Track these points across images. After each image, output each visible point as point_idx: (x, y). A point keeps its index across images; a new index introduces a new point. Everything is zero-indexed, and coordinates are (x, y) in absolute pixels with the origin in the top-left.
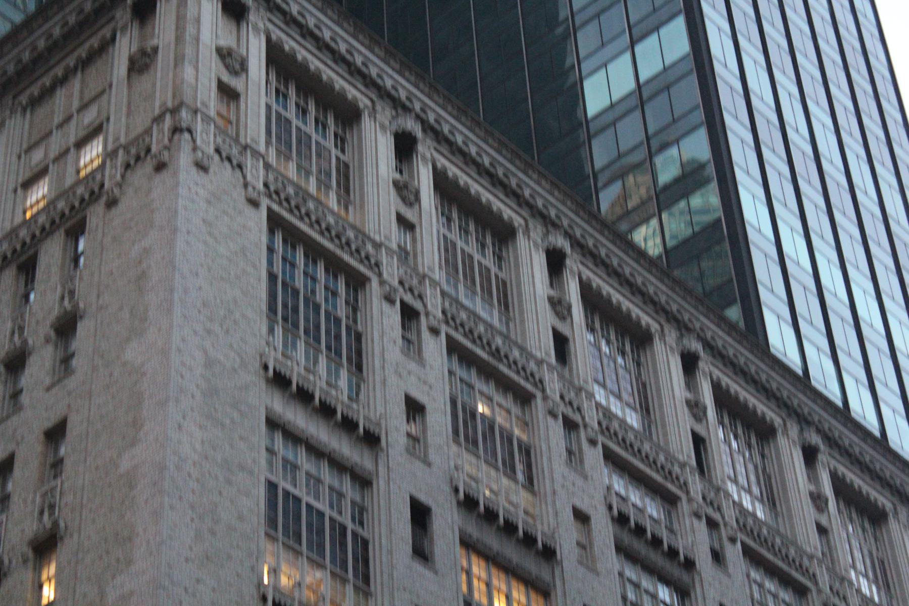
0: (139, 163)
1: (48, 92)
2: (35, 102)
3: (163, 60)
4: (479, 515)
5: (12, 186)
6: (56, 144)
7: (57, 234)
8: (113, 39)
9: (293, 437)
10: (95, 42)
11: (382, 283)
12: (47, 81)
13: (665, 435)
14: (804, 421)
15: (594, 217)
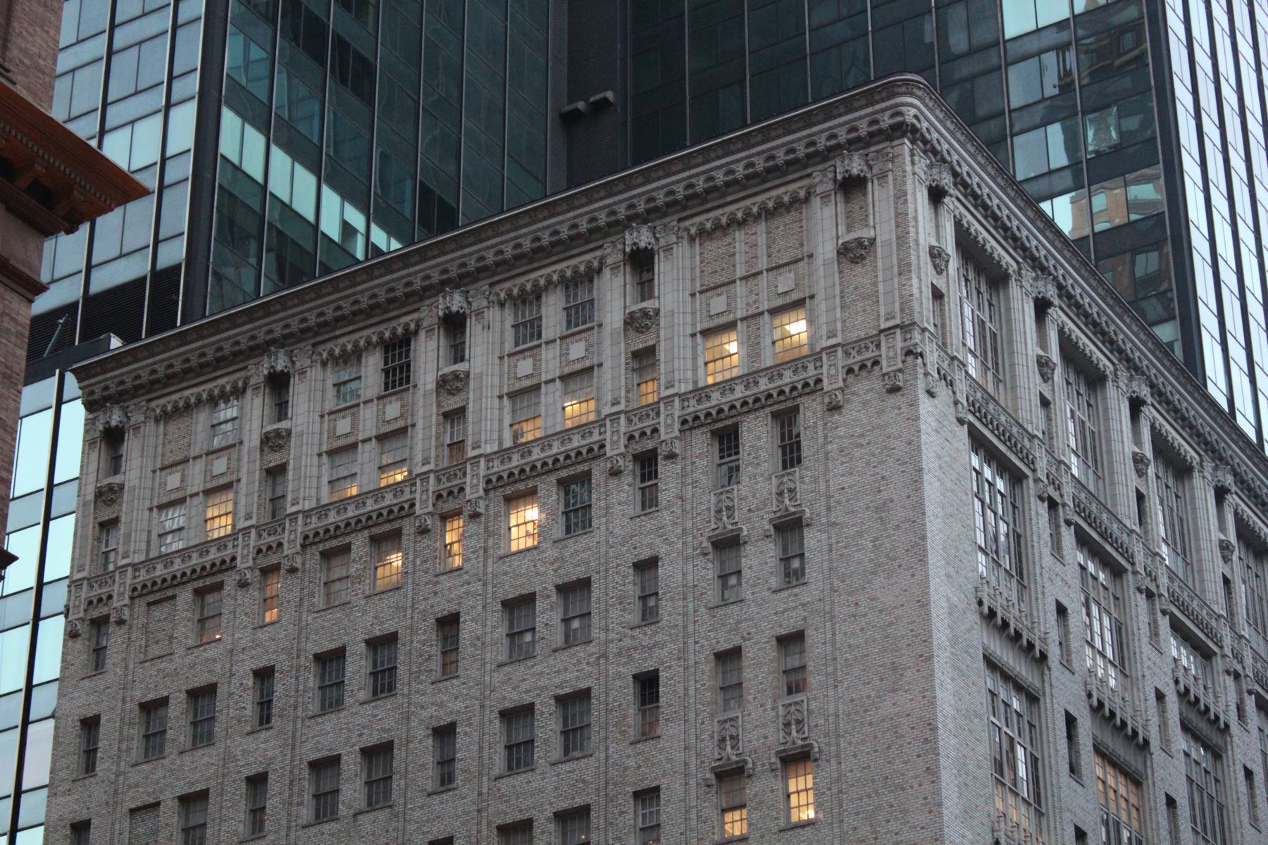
0: (864, 373)
1: (720, 229)
2: (703, 235)
3: (884, 257)
4: (1008, 636)
5: (689, 331)
6: (742, 300)
7: (761, 413)
8: (807, 199)
9: (1007, 677)
10: (784, 193)
11: (1037, 480)
12: (722, 215)
13: (1202, 581)
14: (1220, 459)
15: (1004, 172)
